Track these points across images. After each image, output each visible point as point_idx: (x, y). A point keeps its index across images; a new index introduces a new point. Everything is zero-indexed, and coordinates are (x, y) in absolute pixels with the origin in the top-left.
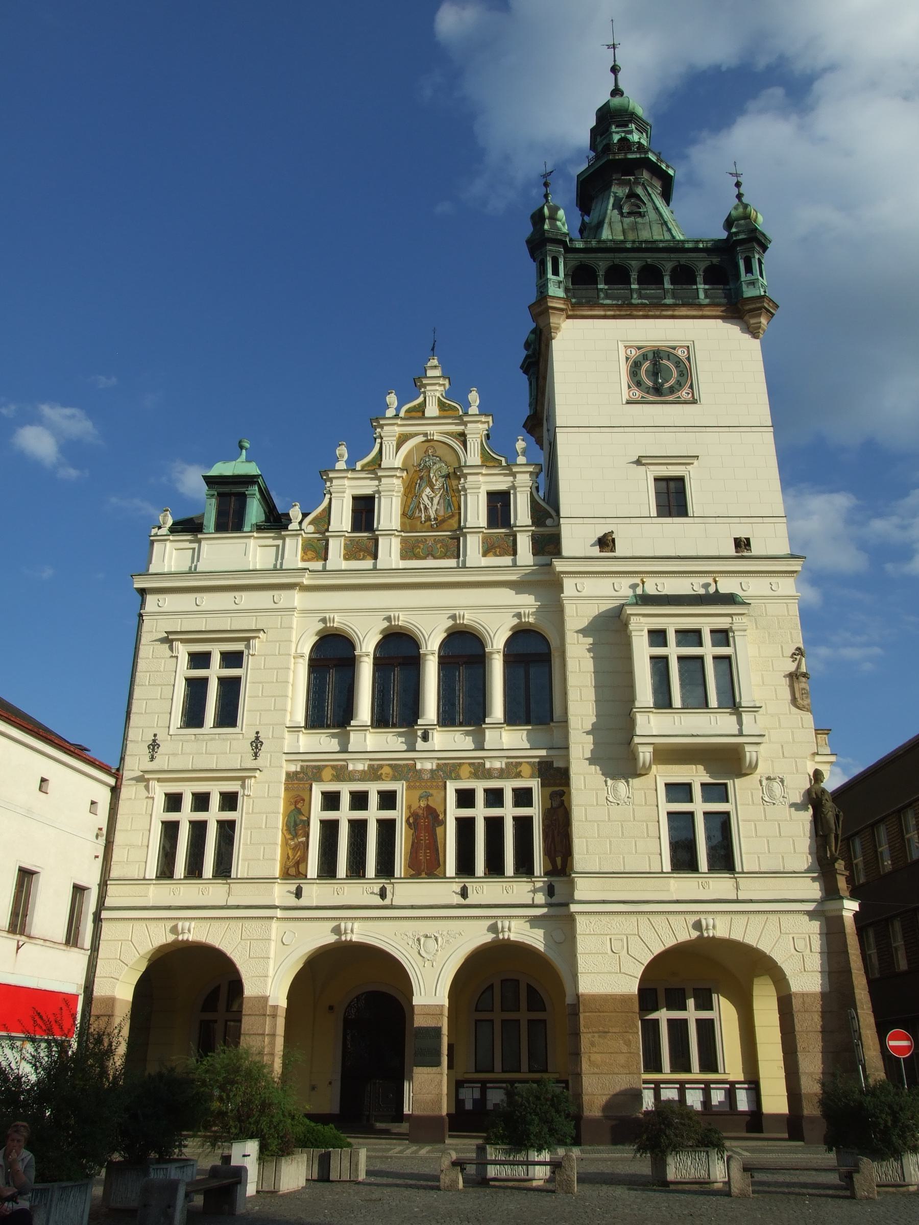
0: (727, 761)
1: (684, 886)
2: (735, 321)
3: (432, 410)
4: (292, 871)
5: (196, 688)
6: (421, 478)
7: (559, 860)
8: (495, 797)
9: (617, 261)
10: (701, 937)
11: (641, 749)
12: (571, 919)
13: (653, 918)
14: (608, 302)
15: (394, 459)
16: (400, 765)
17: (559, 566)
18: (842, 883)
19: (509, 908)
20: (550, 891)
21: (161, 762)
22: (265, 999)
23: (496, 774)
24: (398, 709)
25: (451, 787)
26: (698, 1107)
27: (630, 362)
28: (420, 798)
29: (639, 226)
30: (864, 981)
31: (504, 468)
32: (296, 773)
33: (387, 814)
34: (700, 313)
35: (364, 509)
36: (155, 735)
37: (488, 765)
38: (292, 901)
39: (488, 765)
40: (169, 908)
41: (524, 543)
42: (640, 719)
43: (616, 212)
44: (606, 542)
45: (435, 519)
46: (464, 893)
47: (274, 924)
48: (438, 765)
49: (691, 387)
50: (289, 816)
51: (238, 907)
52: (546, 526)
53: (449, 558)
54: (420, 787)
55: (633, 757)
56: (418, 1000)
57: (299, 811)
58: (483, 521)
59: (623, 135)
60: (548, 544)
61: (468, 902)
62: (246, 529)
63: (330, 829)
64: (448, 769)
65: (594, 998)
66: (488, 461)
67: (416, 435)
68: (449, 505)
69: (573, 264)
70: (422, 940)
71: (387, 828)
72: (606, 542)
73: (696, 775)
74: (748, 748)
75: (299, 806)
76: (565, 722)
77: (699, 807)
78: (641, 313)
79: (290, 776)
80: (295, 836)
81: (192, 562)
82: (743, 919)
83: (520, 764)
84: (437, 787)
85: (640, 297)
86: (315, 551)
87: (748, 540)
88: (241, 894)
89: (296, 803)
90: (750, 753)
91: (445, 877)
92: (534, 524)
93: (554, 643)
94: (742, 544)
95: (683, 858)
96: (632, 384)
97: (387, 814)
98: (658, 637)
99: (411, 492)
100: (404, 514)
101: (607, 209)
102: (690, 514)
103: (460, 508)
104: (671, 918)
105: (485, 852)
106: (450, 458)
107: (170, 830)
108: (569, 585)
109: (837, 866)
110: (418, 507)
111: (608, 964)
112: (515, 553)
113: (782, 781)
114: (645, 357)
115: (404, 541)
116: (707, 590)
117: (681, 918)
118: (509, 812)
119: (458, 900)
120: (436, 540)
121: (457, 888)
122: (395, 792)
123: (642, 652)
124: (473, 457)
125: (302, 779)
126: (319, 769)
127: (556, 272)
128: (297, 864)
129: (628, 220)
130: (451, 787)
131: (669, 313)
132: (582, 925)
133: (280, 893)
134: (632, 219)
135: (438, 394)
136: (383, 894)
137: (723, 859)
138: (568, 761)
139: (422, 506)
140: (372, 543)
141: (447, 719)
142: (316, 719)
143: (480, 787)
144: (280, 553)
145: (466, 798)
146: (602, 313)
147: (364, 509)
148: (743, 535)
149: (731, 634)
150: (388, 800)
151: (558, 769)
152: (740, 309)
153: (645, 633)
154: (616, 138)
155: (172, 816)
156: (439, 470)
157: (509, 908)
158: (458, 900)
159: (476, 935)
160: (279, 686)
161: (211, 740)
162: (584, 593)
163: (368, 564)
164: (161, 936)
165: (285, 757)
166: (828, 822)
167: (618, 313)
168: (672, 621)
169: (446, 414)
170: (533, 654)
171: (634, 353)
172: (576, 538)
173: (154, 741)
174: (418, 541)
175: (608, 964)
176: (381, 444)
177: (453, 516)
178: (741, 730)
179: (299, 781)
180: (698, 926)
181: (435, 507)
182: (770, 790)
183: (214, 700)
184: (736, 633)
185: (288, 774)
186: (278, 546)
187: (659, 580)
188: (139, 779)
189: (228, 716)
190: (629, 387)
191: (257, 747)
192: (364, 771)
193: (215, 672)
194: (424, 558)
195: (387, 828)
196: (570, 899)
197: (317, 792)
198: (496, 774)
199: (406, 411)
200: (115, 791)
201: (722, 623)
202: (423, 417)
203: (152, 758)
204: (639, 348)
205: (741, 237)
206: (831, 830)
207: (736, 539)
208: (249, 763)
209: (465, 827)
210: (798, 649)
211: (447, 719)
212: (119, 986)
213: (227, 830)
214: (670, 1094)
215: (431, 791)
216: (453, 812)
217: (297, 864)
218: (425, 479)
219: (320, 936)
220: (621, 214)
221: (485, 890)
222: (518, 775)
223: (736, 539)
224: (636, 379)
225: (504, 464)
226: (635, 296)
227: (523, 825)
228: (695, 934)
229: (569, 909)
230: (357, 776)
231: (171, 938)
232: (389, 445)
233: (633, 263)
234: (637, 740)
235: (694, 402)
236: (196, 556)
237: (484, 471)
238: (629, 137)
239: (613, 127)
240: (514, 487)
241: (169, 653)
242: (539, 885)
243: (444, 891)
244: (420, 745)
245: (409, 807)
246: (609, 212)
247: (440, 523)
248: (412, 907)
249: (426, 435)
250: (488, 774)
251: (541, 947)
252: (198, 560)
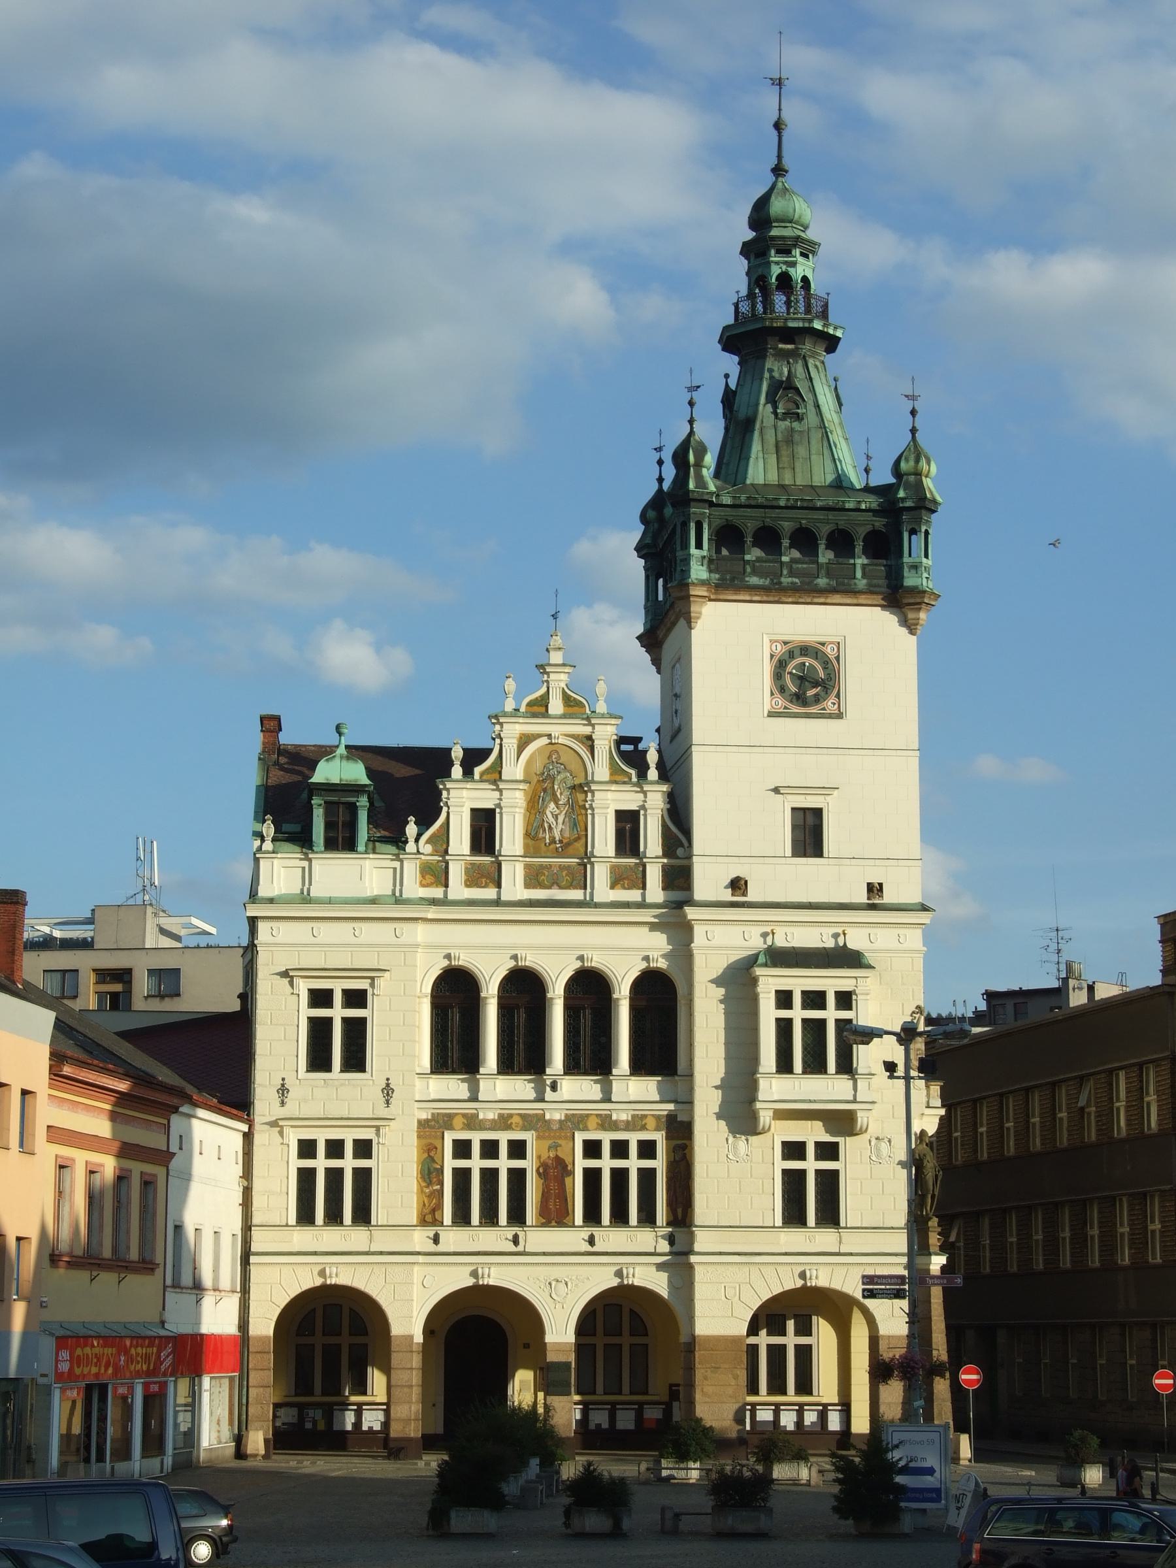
0: (842, 1121)
1: (794, 1238)
2: (895, 610)
3: (556, 706)
4: (429, 1218)
5: (319, 1031)
6: (545, 790)
7: (680, 1211)
8: (620, 1149)
9: (768, 522)
10: (804, 1287)
11: (762, 1113)
12: (690, 1267)
13: (764, 1269)
14: (754, 580)
15: (514, 769)
16: (529, 1115)
17: (691, 913)
18: (934, 1239)
19: (633, 1256)
20: (671, 1240)
21: (291, 1109)
22: (412, 1337)
23: (622, 1126)
24: (524, 1055)
25: (580, 1138)
26: (791, 1427)
27: (776, 659)
28: (550, 1148)
29: (796, 437)
30: (943, 1326)
31: (634, 785)
32: (427, 1121)
33: (517, 1164)
34: (855, 601)
35: (484, 828)
36: (283, 1079)
37: (614, 1117)
38: (432, 1248)
39: (614, 1117)
40: (315, 1253)
41: (654, 875)
42: (763, 1084)
43: (769, 408)
44: (738, 885)
45: (561, 842)
46: (591, 1241)
47: (416, 1268)
48: (566, 1115)
49: (838, 696)
50: (423, 1164)
51: (381, 1253)
52: (678, 858)
53: (575, 888)
54: (549, 1137)
55: (754, 1116)
56: (549, 1338)
57: (433, 1160)
58: (611, 850)
59: (784, 267)
60: (679, 877)
61: (595, 1249)
62: (361, 847)
63: (461, 1177)
64: (576, 1122)
65: (709, 1339)
66: (617, 777)
67: (539, 736)
68: (575, 825)
69: (717, 522)
70: (554, 1284)
71: (517, 1177)
72: (738, 885)
73: (813, 1133)
74: (859, 1114)
75: (432, 1154)
76: (690, 1075)
77: (811, 1165)
78: (790, 600)
79: (422, 1124)
80: (430, 1184)
81: (303, 884)
82: (843, 1270)
83: (645, 1116)
84: (566, 1138)
85: (791, 574)
86: (434, 875)
87: (881, 885)
88: (383, 1240)
89: (429, 1151)
90: (862, 1119)
91: (574, 1226)
92: (665, 855)
93: (681, 990)
94: (874, 889)
95: (794, 1215)
96: (776, 691)
97: (517, 1164)
98: (784, 999)
99: (535, 807)
100: (527, 834)
101: (757, 404)
102: (825, 854)
103: (586, 830)
104: (779, 1269)
105: (609, 1201)
106: (574, 765)
107: (306, 1178)
108: (699, 931)
109: (930, 1224)
110: (542, 825)
111: (721, 1308)
112: (644, 887)
113: (890, 1141)
114: (791, 654)
115: (527, 867)
116: (836, 942)
117: (789, 1268)
118: (633, 1164)
119: (586, 1247)
120: (562, 868)
121: (585, 1233)
122: (525, 1141)
123: (769, 1014)
124: (601, 770)
125: (433, 1127)
126: (450, 1117)
127: (699, 546)
128: (433, 1211)
129: (783, 425)
130: (580, 1138)
131: (822, 600)
132: (700, 1274)
133: (420, 1239)
134: (787, 423)
135: (563, 685)
136: (516, 1240)
137: (830, 1215)
138: (692, 1117)
139: (546, 825)
140: (494, 869)
141: (573, 1067)
142: (442, 1063)
143: (606, 1138)
144: (398, 877)
145: (592, 1148)
146: (748, 598)
147: (484, 828)
148: (875, 880)
149: (854, 997)
150: (517, 1149)
151: (682, 1122)
152: (899, 597)
153: (773, 992)
154: (775, 271)
155: (308, 1163)
156: (564, 781)
157: (633, 1256)
158: (586, 1247)
159: (601, 1280)
160: (403, 1028)
161: (342, 1085)
162: (714, 943)
163: (490, 893)
164: (308, 1280)
165: (417, 1105)
166: (926, 1182)
167: (765, 598)
168: (800, 981)
169: (571, 710)
170: (660, 996)
171: (779, 649)
172: (708, 881)
173: (283, 1085)
174: (542, 867)
175: (721, 1308)
176: (501, 745)
177: (578, 839)
178: (855, 1096)
179: (432, 1128)
180: (803, 1275)
181: (560, 826)
182: (878, 1150)
183: (340, 1043)
184: (860, 997)
185: (419, 1122)
186: (395, 869)
187: (789, 929)
188: (274, 1124)
189: (355, 1060)
190: (772, 694)
191: (388, 1094)
192: (493, 1120)
193: (338, 1013)
194: (549, 888)
195: (517, 1177)
196: (691, 1252)
197: (449, 1137)
198: (622, 1126)
199: (529, 704)
200: (248, 1137)
201: (845, 985)
202: (545, 715)
203: (283, 1103)
204: (785, 643)
205: (909, 504)
206: (928, 1191)
207: (869, 884)
208: (382, 1112)
209: (593, 1177)
210: (918, 1007)
211: (573, 1067)
212: (263, 1325)
213: (363, 1178)
214: (765, 1415)
215: (560, 1142)
216: (581, 1163)
217: (433, 1211)
218: (549, 791)
219: (457, 1279)
220: (775, 413)
221: (611, 1238)
222: (643, 1128)
223: (869, 884)
224: (780, 683)
225: (634, 779)
226: (785, 572)
227: (648, 1177)
228: (799, 1283)
229: (688, 1259)
230: (488, 1125)
231: (319, 1282)
232: (510, 745)
233: (786, 524)
234: (758, 1105)
235: (839, 716)
236: (307, 876)
237: (614, 787)
238: (791, 271)
239: (773, 252)
240: (643, 807)
241: (288, 989)
242: (660, 1234)
243: (573, 1238)
244: (549, 1095)
245: (539, 1157)
246: (761, 407)
247: (564, 848)
248: (544, 1254)
249: (549, 736)
250: (614, 1126)
251: (664, 1293)
252: (310, 884)
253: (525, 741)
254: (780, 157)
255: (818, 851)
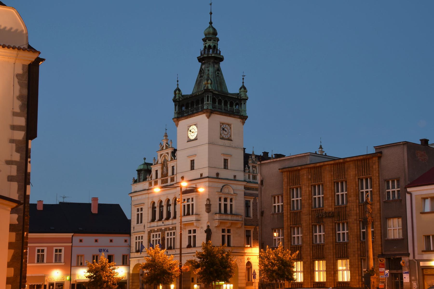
14: (185, 115)
64: (166, 229)
99: (162, 168)
174: (163, 180)
179: (150, 233)
253: (161, 155)
254: (211, 23)
255: (193, 169)
